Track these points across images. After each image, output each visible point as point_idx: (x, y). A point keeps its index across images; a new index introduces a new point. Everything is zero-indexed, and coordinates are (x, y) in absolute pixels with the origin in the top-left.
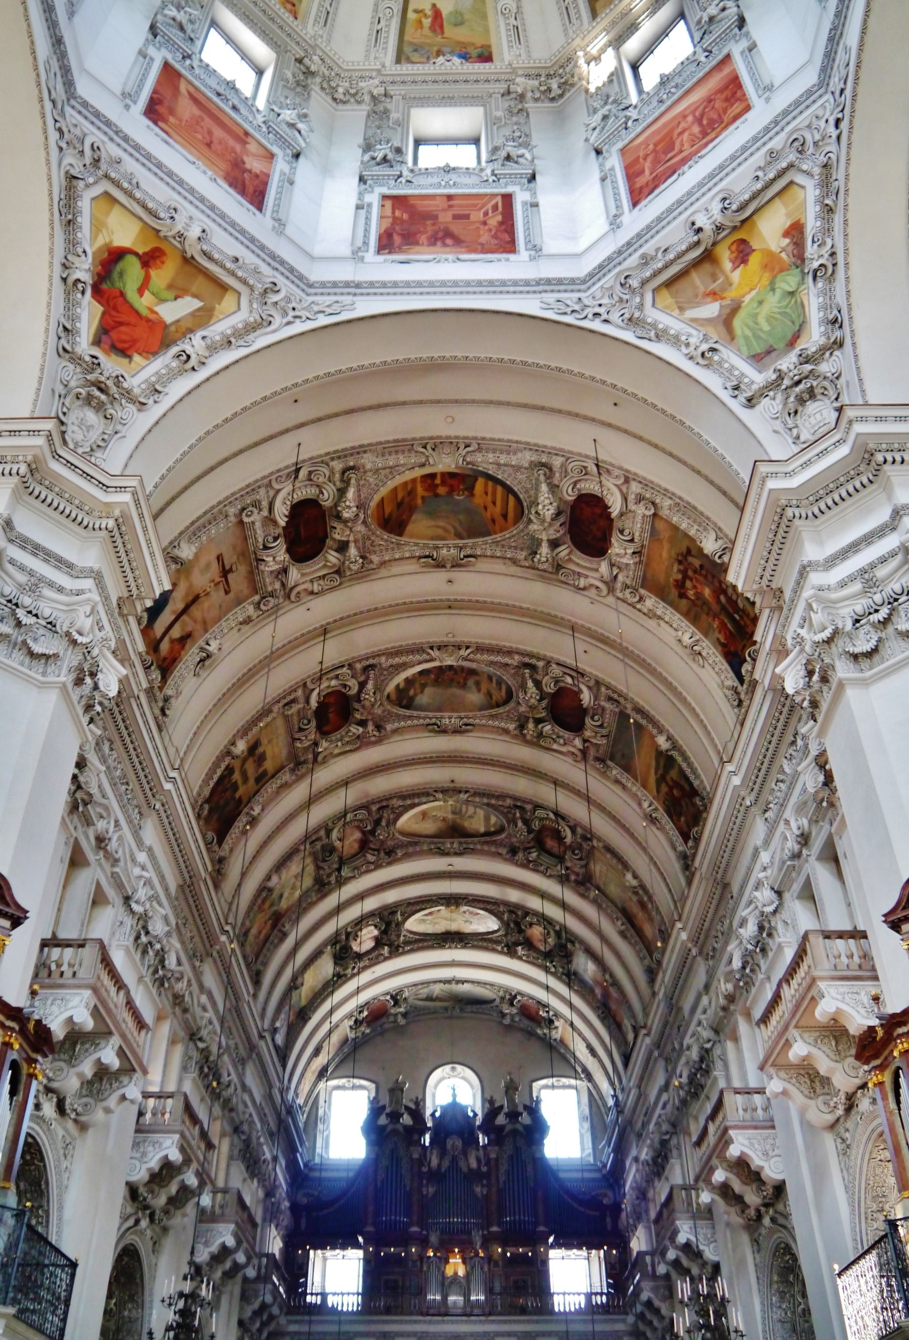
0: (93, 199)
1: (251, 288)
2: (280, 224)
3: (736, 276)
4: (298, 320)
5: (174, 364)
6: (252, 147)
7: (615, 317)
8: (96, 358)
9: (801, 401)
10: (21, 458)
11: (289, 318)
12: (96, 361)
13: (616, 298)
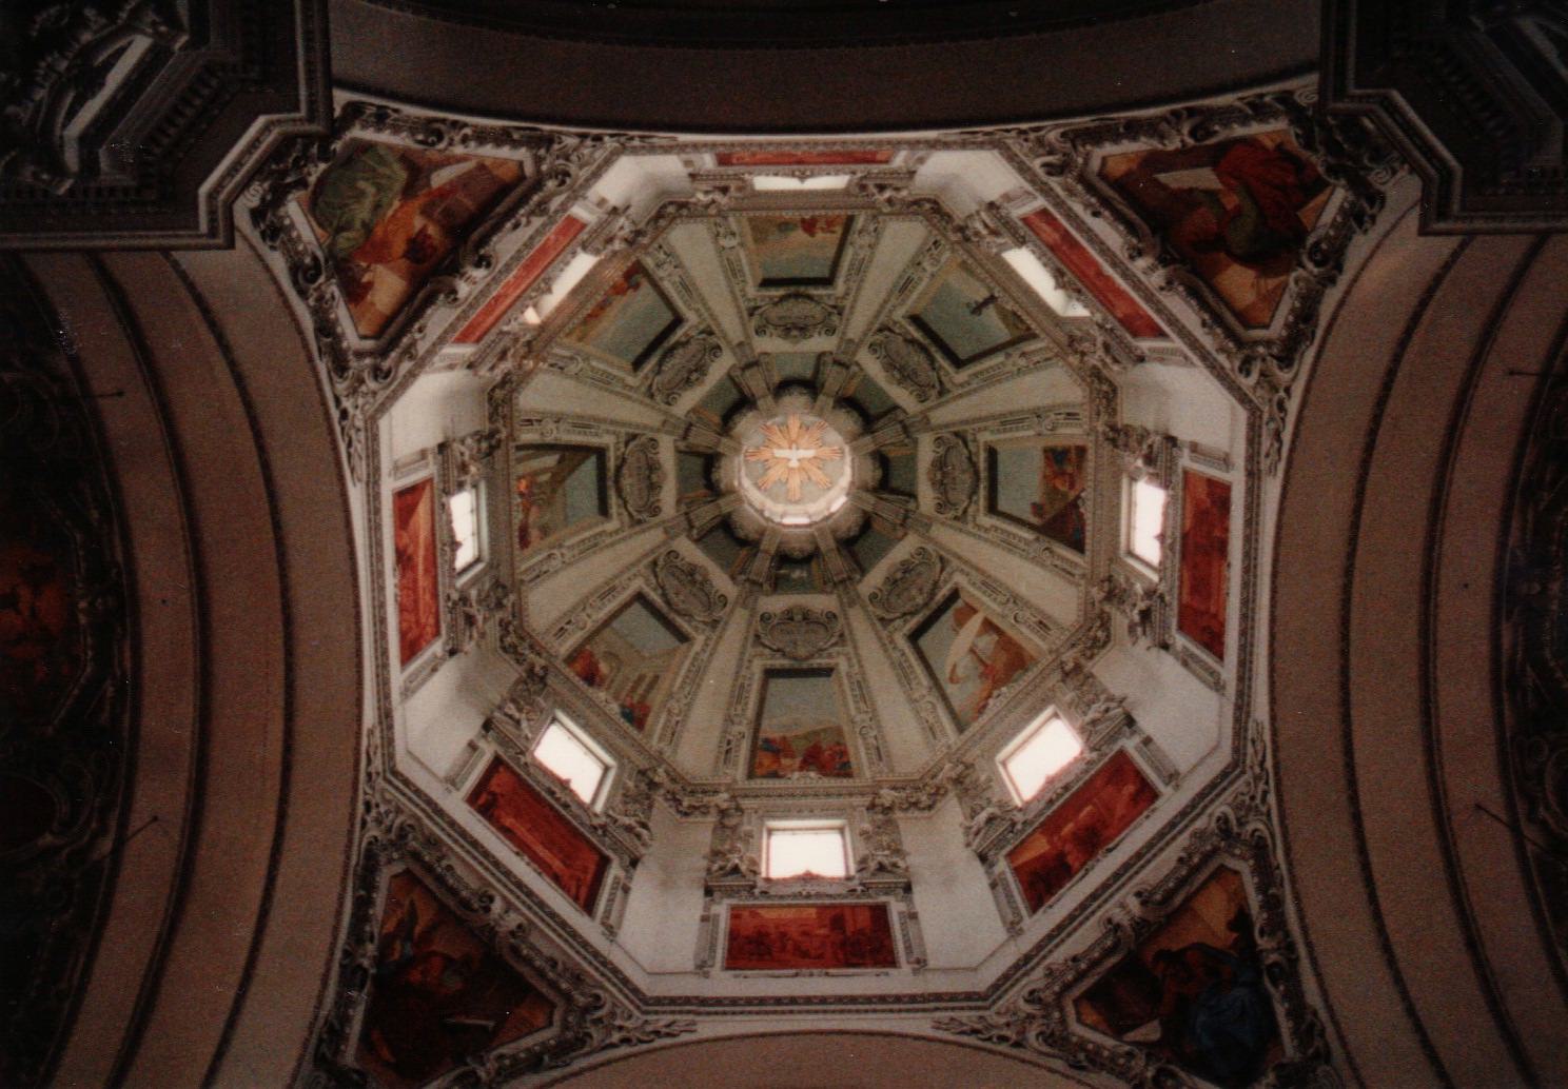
0: (1267, 327)
3: (418, 222)
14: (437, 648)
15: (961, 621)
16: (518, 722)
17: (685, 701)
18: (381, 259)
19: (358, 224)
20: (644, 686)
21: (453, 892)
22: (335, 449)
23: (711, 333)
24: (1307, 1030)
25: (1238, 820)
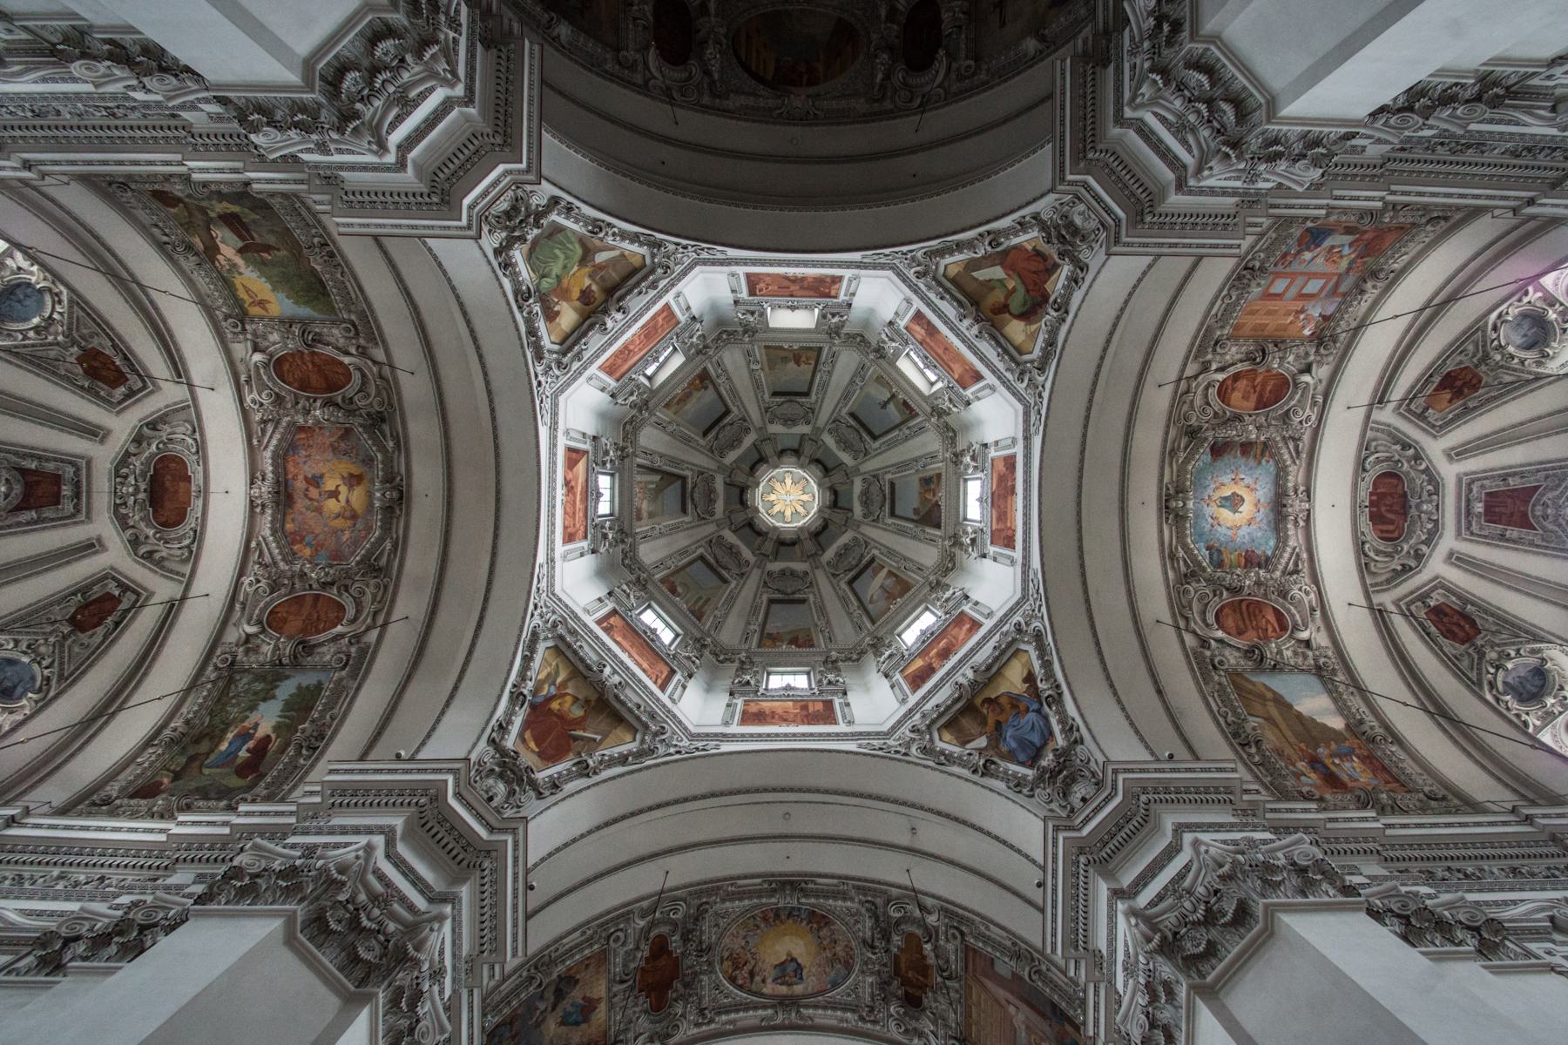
3: (587, 282)
14: (585, 544)
16: (628, 595)
19: (554, 273)
21: (582, 660)
22: (533, 401)
24: (1069, 729)
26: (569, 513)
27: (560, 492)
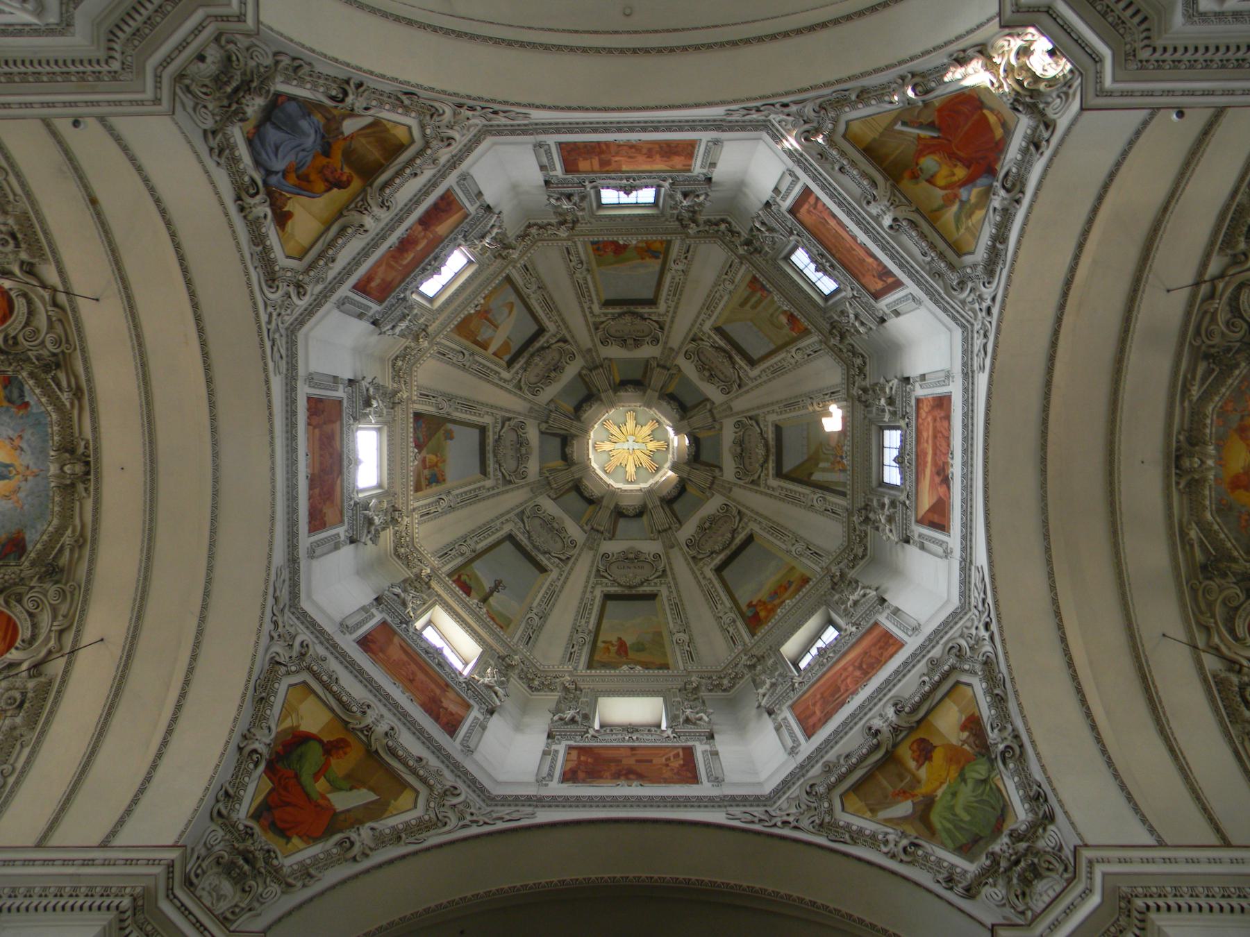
0: (291, 686)
1: (431, 787)
2: (468, 750)
3: (923, 773)
4: (475, 825)
5: (335, 851)
6: (451, 695)
7: (805, 823)
8: (251, 829)
9: (1026, 882)
10: (128, 890)
11: (466, 822)
12: (250, 831)
13: (804, 807)
15: (506, 345)
16: (857, 317)
17: (721, 288)
18: (950, 748)
20: (754, 300)
23: (694, 558)
25: (290, 297)
26: (943, 437)
27: (956, 470)
